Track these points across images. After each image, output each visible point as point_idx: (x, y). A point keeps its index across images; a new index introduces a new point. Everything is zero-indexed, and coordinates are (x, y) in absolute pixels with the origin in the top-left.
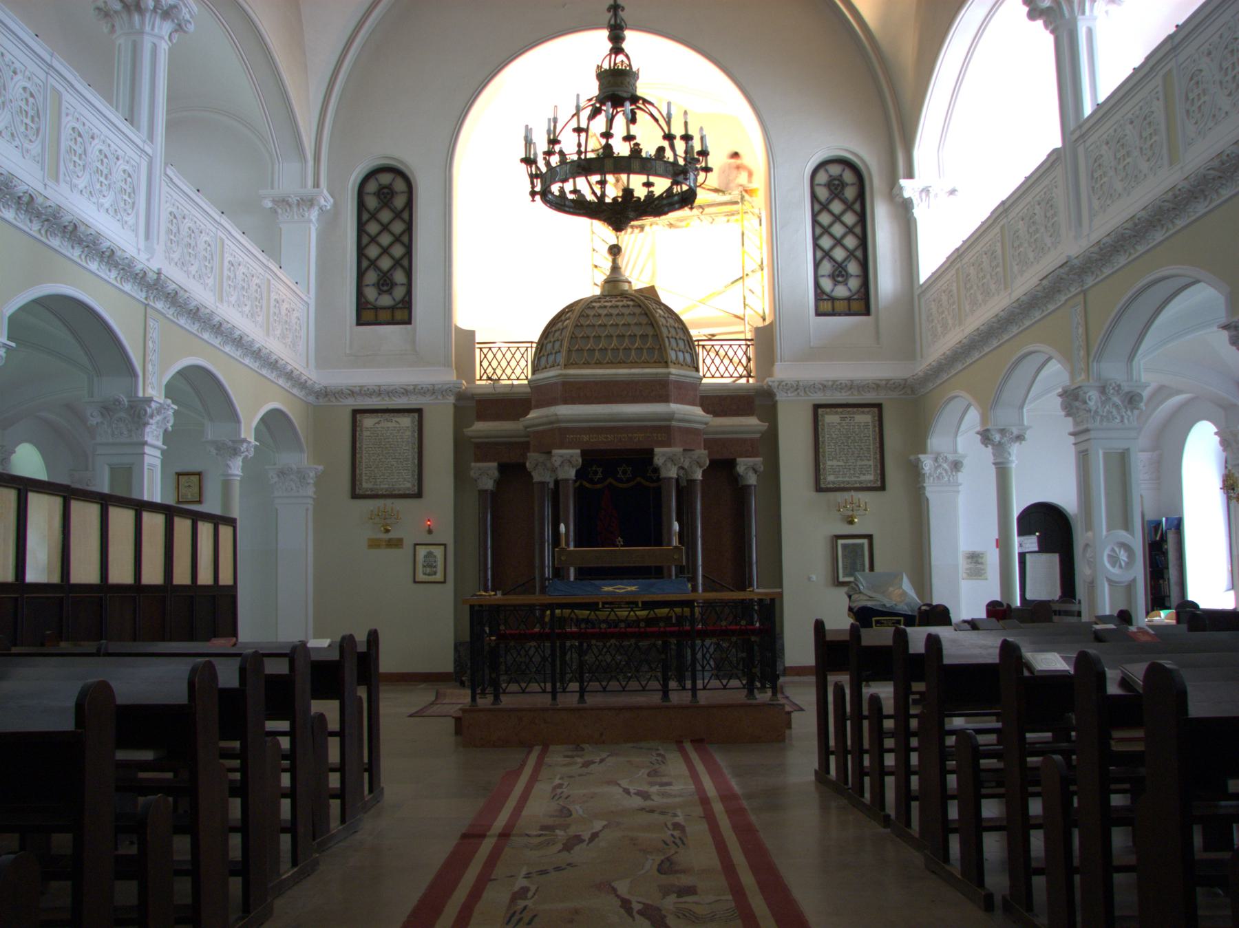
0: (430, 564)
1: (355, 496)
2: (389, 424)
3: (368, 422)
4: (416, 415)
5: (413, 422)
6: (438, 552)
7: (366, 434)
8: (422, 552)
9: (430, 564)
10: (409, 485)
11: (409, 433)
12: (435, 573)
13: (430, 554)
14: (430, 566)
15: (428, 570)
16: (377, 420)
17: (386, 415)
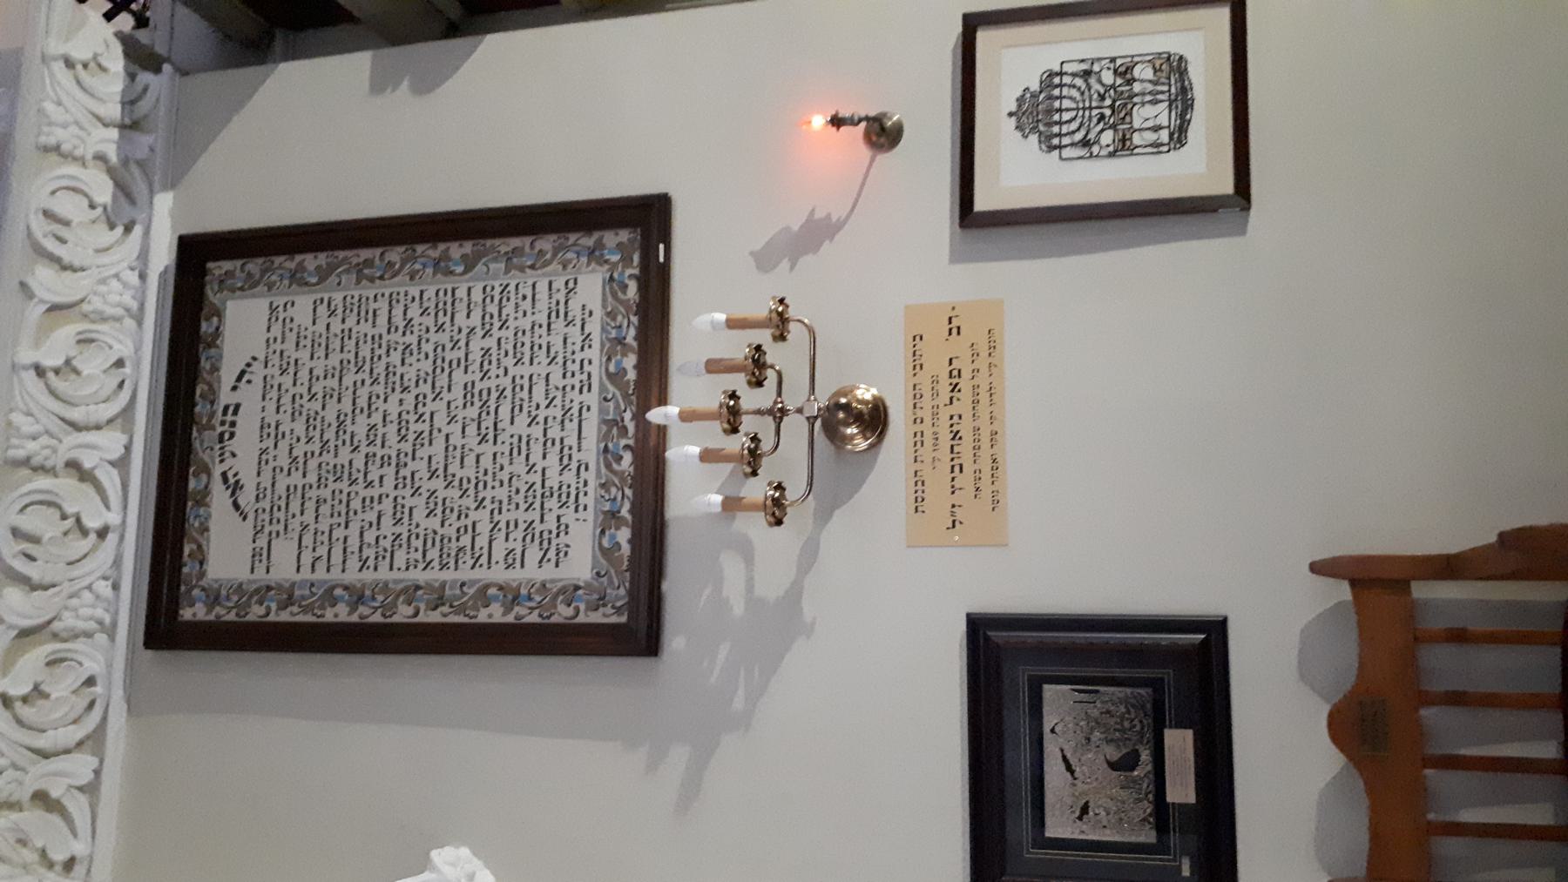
0: (1094, 111)
1: (639, 634)
2: (247, 425)
3: (225, 553)
4: (218, 268)
5: (251, 283)
6: (1014, 64)
7: (283, 567)
8: (1017, 172)
9: (1094, 111)
10: (591, 287)
11: (303, 305)
12: (1174, 67)
13: (1037, 114)
14: (1119, 108)
15: (1151, 115)
16: (219, 497)
17: (203, 443)
